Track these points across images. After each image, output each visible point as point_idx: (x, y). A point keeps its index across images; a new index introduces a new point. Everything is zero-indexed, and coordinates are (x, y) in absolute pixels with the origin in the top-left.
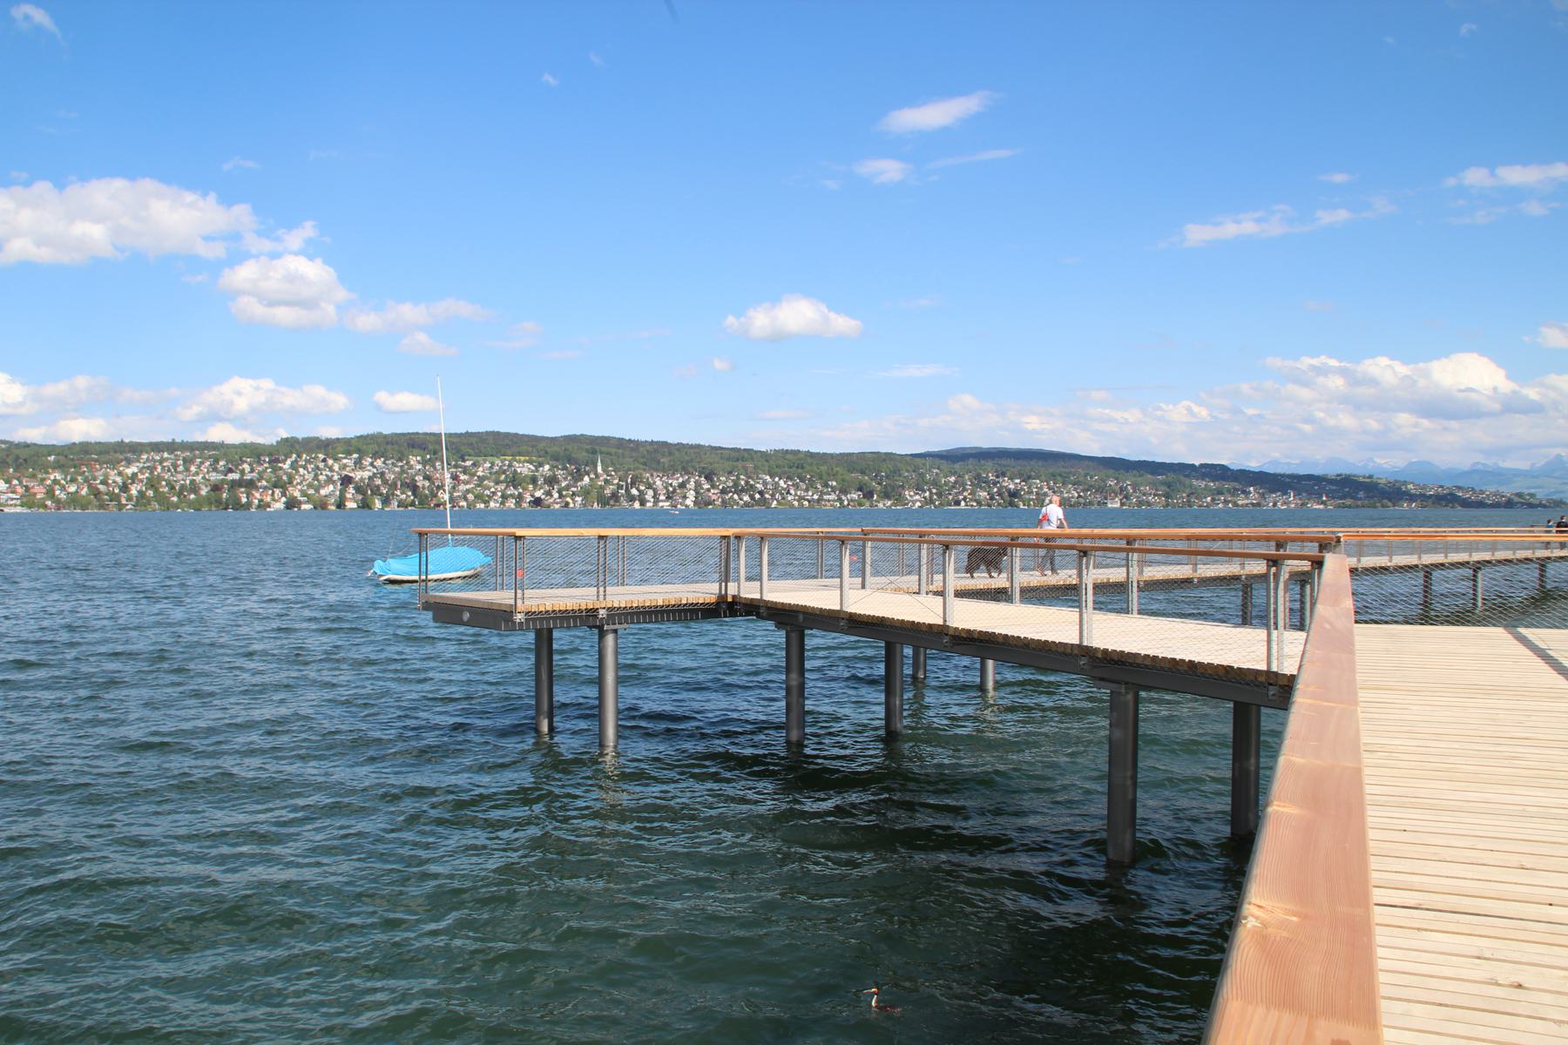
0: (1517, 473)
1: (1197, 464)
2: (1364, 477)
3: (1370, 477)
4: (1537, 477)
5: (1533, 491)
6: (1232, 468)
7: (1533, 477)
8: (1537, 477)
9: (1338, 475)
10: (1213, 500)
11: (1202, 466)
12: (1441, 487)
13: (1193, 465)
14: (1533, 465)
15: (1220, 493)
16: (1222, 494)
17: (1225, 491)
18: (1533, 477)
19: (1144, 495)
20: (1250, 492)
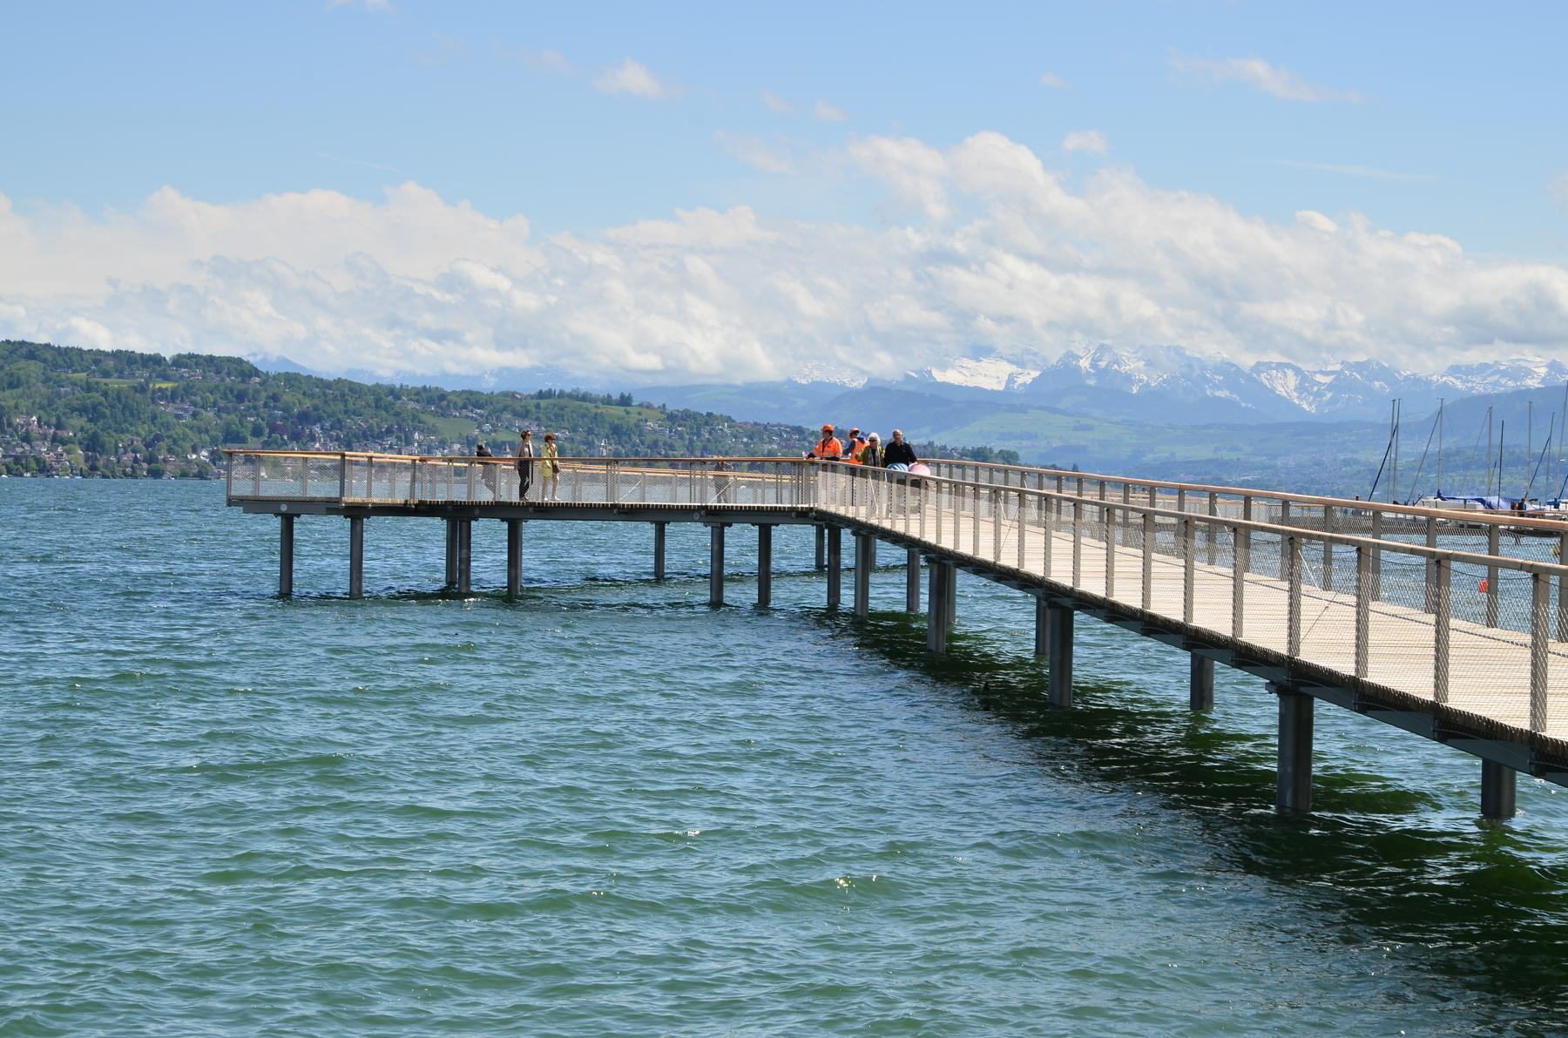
0: (976, 402)
1: (168, 354)
2: (608, 401)
3: (625, 401)
4: (1022, 409)
5: (1010, 446)
6: (262, 369)
7: (1012, 408)
8: (1022, 409)
9: (541, 395)
10: (215, 457)
11: (179, 361)
12: (799, 430)
13: (154, 361)
14: (1011, 379)
15: (232, 437)
16: (243, 440)
17: (246, 433)
18: (1012, 408)
19: (27, 439)
20: (313, 438)
